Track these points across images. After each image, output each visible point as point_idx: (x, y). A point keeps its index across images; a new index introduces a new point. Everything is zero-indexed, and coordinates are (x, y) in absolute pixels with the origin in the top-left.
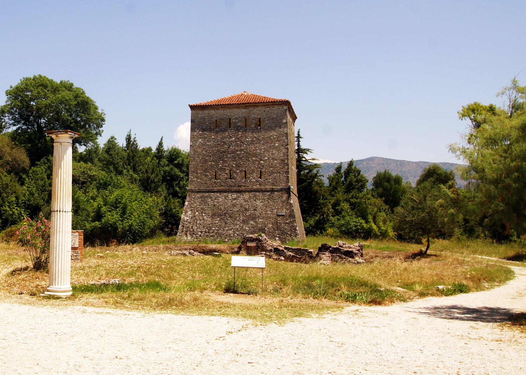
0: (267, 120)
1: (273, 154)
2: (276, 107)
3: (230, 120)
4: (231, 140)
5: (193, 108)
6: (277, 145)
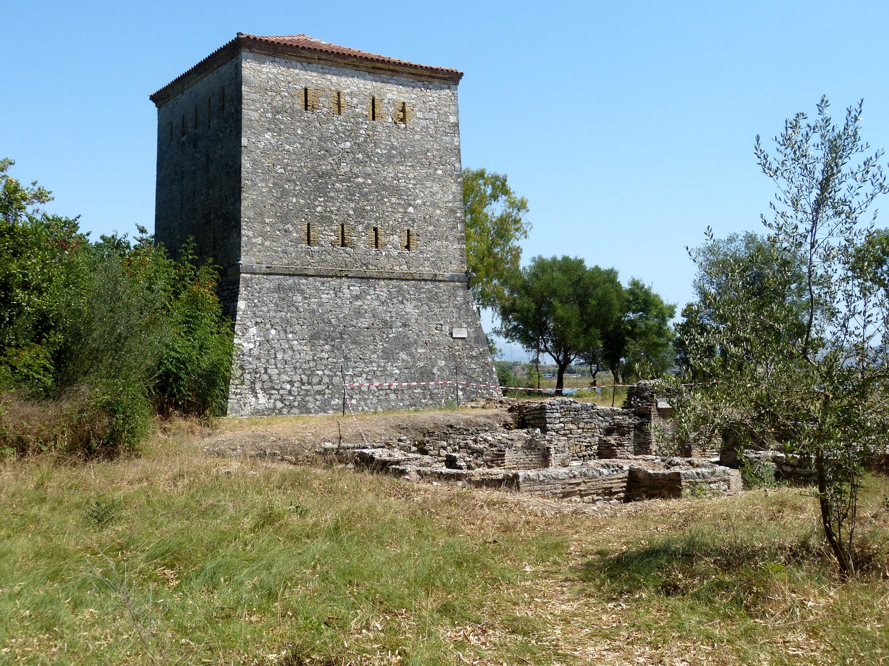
1: (433, 194)
3: (339, 94)
4: (342, 146)
6: (440, 172)
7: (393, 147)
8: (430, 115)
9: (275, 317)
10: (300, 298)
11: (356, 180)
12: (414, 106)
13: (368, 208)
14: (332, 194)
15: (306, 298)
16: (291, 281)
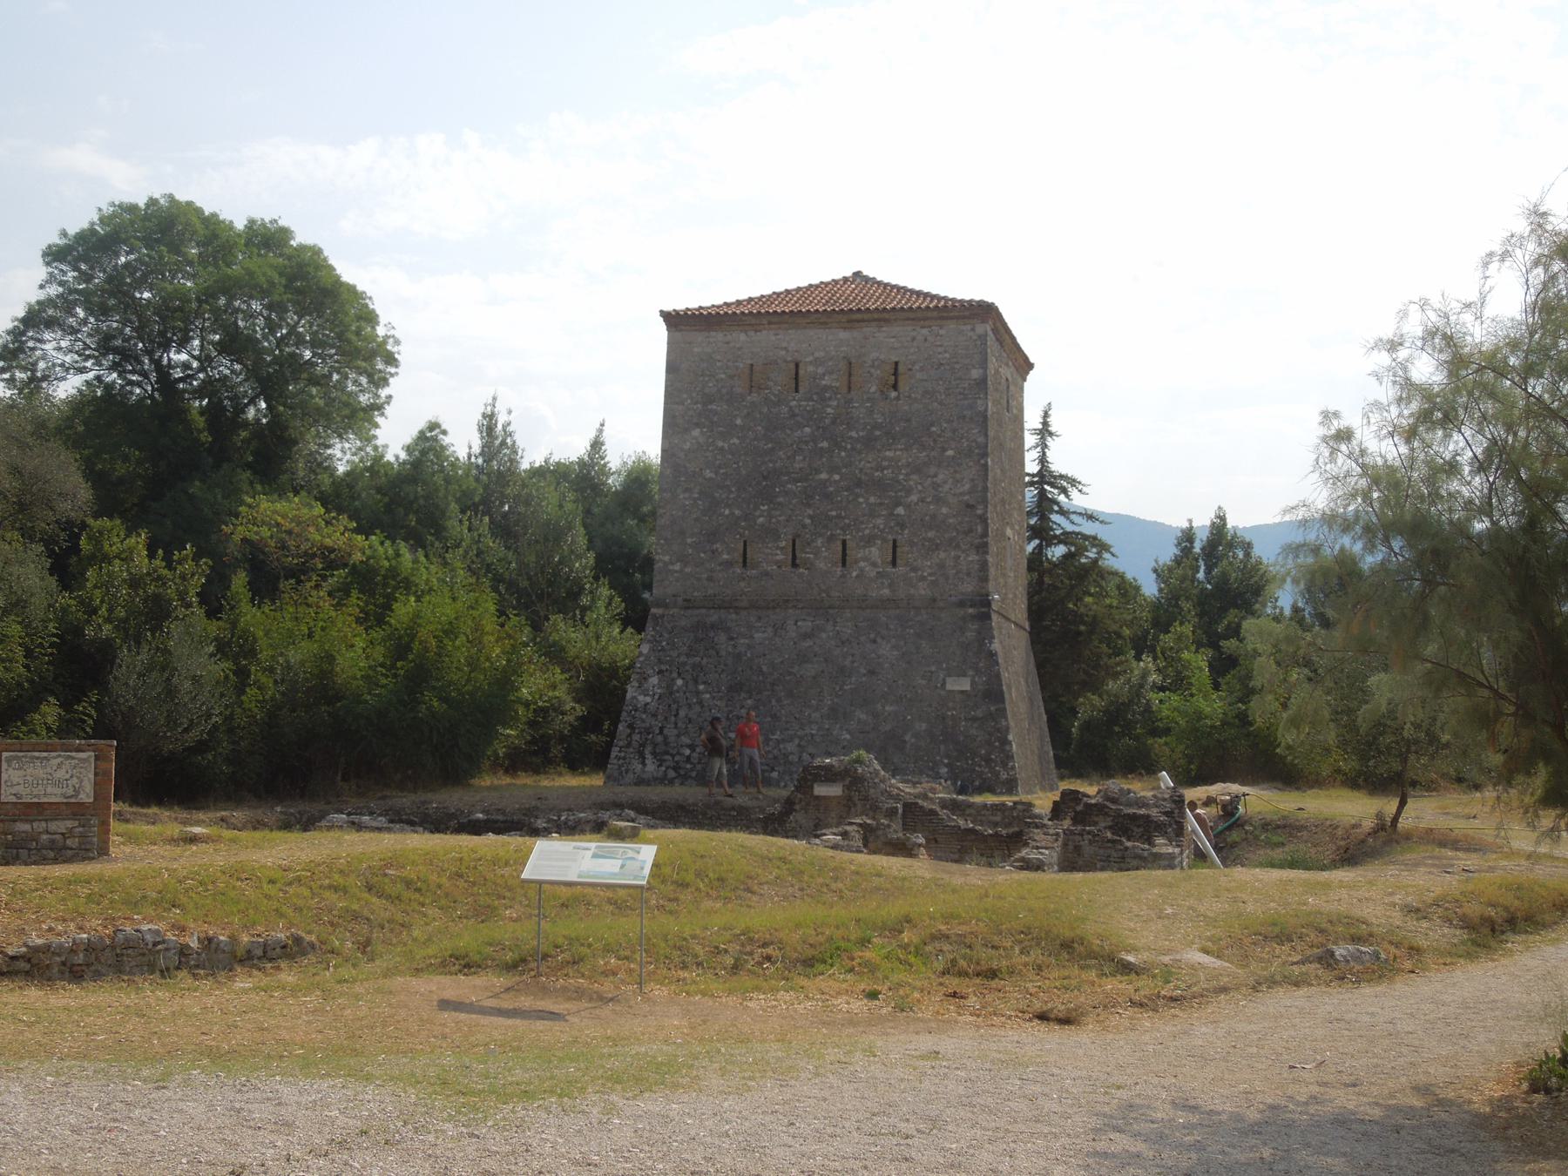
0: (922, 369)
1: (936, 486)
2: (952, 325)
3: (797, 366)
5: (675, 321)
6: (950, 453)
7: (876, 426)
9: (685, 664)
10: (722, 637)
12: (914, 364)
14: (781, 499)
15: (732, 639)
16: (714, 617)
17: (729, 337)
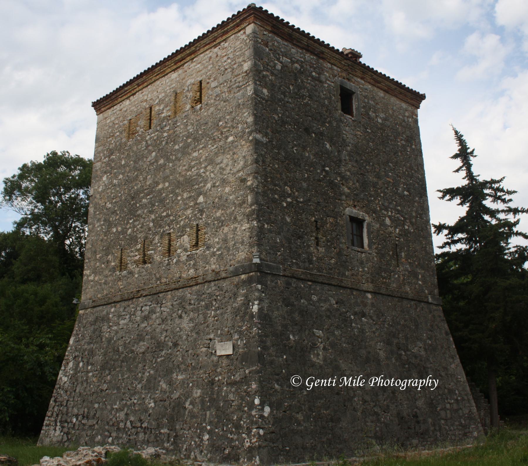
3: (151, 108)
6: (231, 139)
8: (225, 78)
11: (158, 188)
13: (165, 214)
14: (139, 212)
17: (121, 107)
